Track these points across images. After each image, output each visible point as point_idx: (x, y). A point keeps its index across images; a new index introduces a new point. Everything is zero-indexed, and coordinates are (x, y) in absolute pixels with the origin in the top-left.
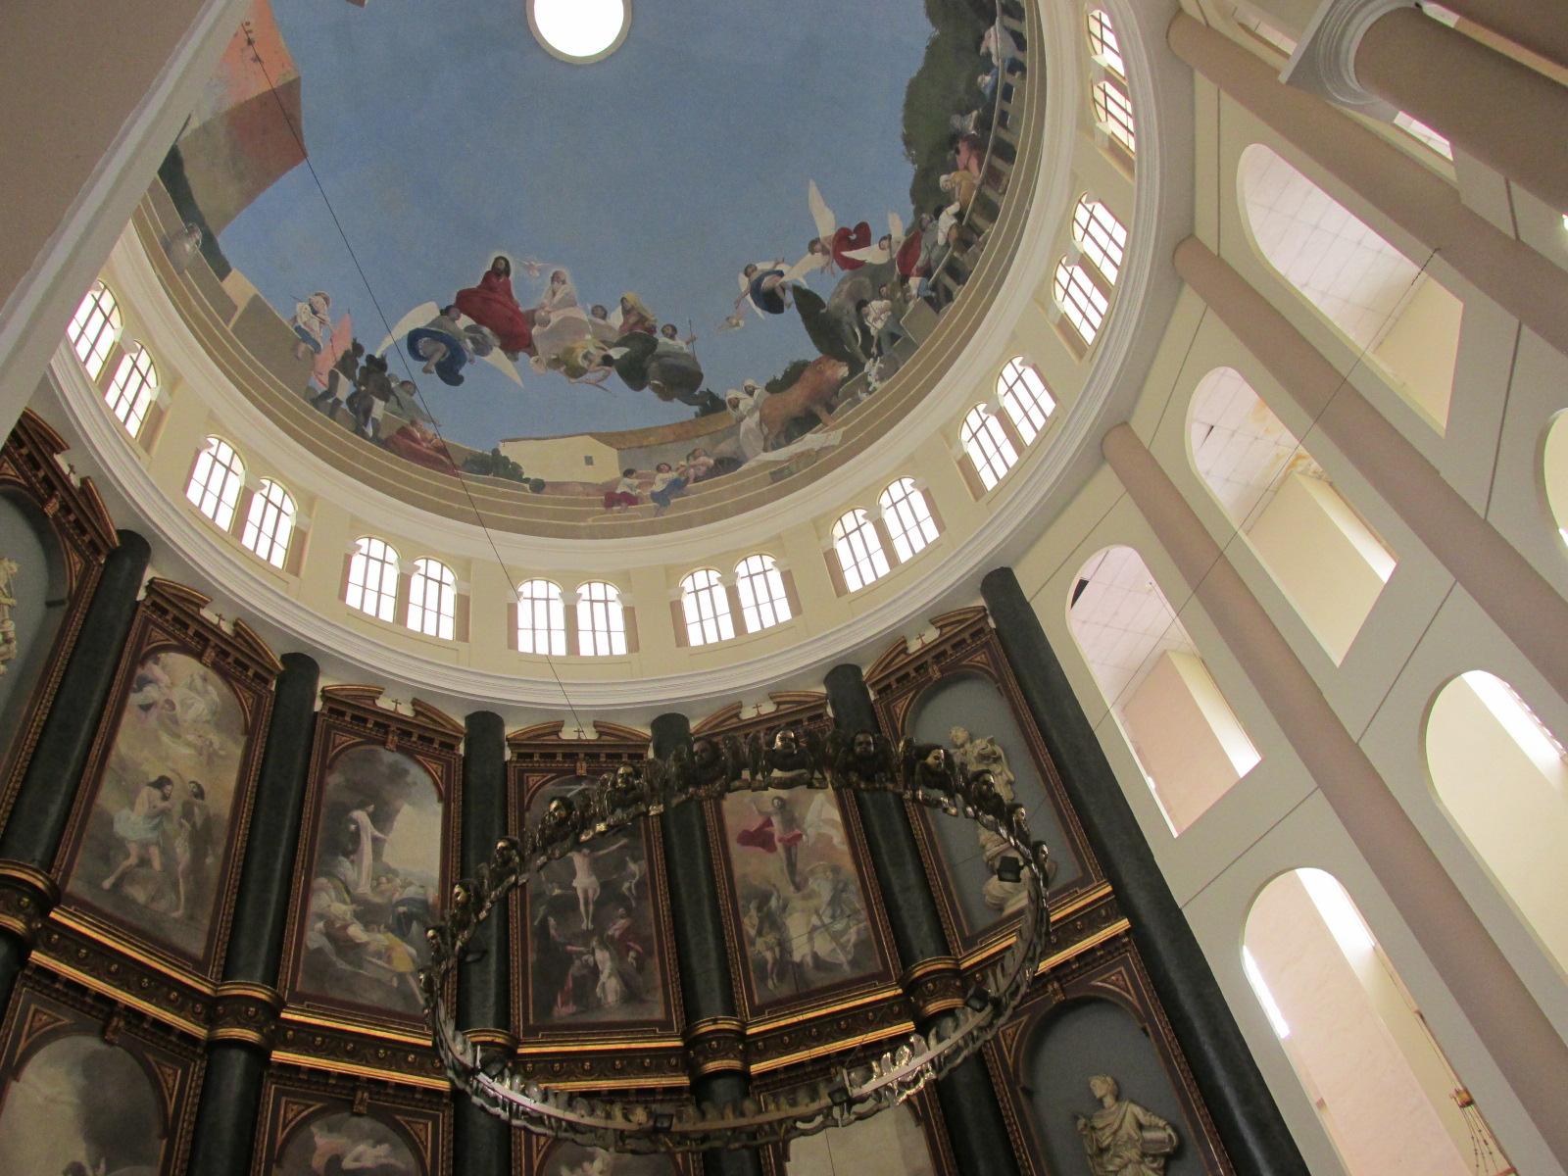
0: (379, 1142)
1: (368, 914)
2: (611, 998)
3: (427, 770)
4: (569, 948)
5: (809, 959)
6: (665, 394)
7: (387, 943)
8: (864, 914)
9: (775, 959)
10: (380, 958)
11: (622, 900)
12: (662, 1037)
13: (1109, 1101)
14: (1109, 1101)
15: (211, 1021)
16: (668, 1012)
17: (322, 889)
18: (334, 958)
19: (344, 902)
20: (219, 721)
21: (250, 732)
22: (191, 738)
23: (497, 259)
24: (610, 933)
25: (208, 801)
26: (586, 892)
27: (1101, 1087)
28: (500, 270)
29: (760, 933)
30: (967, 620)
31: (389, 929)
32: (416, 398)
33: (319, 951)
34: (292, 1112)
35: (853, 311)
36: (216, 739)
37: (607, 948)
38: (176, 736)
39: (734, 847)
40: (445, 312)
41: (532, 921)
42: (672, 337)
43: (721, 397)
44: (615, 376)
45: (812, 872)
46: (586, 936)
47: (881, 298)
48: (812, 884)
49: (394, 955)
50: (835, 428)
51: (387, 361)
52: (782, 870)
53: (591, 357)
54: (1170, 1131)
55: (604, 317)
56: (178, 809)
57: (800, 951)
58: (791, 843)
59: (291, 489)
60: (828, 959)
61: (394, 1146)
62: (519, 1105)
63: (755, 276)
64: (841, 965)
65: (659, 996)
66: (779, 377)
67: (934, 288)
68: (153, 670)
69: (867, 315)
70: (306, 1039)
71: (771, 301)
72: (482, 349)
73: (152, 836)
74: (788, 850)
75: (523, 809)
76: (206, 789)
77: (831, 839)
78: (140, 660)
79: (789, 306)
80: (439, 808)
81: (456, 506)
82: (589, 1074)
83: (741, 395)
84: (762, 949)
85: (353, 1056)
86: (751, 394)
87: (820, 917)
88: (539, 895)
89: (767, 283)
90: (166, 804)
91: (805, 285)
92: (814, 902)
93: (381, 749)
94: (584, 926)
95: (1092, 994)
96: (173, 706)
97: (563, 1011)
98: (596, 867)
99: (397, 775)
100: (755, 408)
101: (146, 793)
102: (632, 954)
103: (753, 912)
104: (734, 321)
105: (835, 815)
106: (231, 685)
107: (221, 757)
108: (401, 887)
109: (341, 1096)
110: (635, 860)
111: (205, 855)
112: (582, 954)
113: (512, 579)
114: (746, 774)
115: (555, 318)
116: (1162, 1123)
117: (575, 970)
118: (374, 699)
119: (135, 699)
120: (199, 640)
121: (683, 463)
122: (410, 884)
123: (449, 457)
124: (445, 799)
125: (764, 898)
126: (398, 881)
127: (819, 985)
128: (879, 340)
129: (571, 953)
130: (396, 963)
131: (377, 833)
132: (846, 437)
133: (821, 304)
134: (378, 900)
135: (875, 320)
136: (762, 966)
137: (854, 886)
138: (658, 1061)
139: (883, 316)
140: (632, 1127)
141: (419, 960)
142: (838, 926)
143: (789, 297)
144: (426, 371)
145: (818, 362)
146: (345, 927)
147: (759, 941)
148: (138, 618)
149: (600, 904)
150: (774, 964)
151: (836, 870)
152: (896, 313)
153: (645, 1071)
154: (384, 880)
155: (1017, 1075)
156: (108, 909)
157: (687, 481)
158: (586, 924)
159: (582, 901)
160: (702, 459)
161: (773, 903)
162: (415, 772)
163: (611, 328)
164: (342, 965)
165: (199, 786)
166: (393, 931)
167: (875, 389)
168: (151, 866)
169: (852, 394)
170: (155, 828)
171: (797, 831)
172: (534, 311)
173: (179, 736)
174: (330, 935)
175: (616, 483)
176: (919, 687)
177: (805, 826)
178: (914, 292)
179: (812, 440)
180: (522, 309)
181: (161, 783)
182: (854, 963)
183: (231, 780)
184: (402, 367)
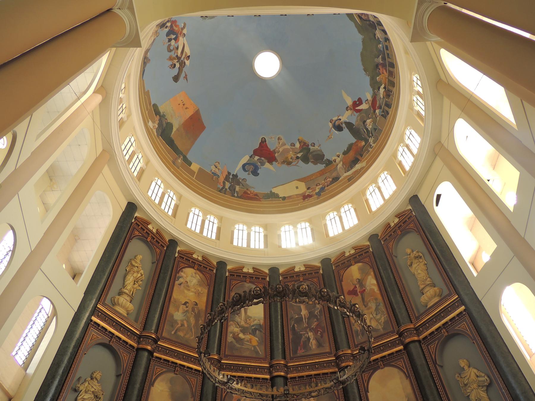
1: (244, 330)
2: (314, 347)
6: (315, 163)
7: (250, 338)
8: (385, 312)
9: (360, 329)
10: (248, 342)
11: (316, 316)
12: (329, 357)
13: (466, 368)
14: (466, 368)
17: (232, 325)
18: (236, 344)
20: (200, 284)
21: (209, 285)
22: (193, 290)
23: (262, 138)
24: (312, 327)
26: (305, 315)
27: (463, 363)
28: (263, 141)
30: (406, 214)
31: (250, 334)
32: (247, 182)
33: (231, 342)
35: (363, 125)
36: (200, 289)
37: (312, 332)
40: (251, 157)
41: (290, 326)
42: (314, 146)
43: (331, 160)
44: (300, 161)
45: (369, 301)
47: (370, 119)
49: (252, 341)
50: (363, 161)
51: (238, 175)
52: (361, 302)
53: (292, 158)
54: (486, 377)
55: (294, 146)
56: (190, 310)
58: (362, 292)
59: (216, 216)
62: (243, 390)
63: (333, 122)
64: (380, 329)
65: (328, 344)
66: (346, 150)
67: (383, 112)
68: (182, 274)
69: (367, 125)
71: (339, 128)
72: (263, 164)
73: (184, 318)
74: (362, 295)
77: (374, 289)
79: (344, 128)
81: (262, 210)
82: (308, 370)
83: (336, 158)
85: (242, 371)
86: (339, 157)
87: (373, 315)
88: (292, 318)
89: (337, 123)
90: (187, 309)
91: (348, 121)
92: (370, 310)
93: (245, 283)
95: (455, 332)
97: (301, 352)
98: (307, 308)
100: (341, 161)
101: (181, 306)
102: (319, 332)
104: (330, 137)
105: (375, 282)
106: (203, 274)
107: (202, 293)
108: (253, 321)
114: (247, 302)
115: (281, 150)
116: (483, 375)
117: (303, 339)
118: (242, 270)
121: (323, 182)
122: (256, 320)
123: (258, 196)
126: (252, 320)
128: (371, 131)
129: (301, 334)
132: (367, 163)
133: (354, 125)
134: (246, 326)
135: (369, 126)
136: (357, 331)
137: (382, 304)
139: (371, 124)
141: (259, 341)
142: (378, 317)
143: (344, 125)
144: (249, 174)
145: (356, 142)
147: (355, 324)
148: (176, 261)
150: (360, 332)
152: (374, 122)
153: (325, 368)
154: (248, 320)
155: (436, 361)
156: (174, 339)
157: (325, 187)
158: (305, 325)
160: (328, 179)
163: (297, 148)
164: (238, 345)
165: (196, 302)
166: (251, 334)
167: (373, 146)
168: (184, 326)
169: (367, 150)
170: (184, 316)
171: (364, 289)
172: (275, 149)
174: (234, 338)
175: (305, 192)
176: (395, 238)
177: (366, 287)
178: (378, 114)
179: (358, 166)
180: (271, 150)
181: (186, 303)
182: (384, 329)
183: (205, 299)
184: (242, 175)
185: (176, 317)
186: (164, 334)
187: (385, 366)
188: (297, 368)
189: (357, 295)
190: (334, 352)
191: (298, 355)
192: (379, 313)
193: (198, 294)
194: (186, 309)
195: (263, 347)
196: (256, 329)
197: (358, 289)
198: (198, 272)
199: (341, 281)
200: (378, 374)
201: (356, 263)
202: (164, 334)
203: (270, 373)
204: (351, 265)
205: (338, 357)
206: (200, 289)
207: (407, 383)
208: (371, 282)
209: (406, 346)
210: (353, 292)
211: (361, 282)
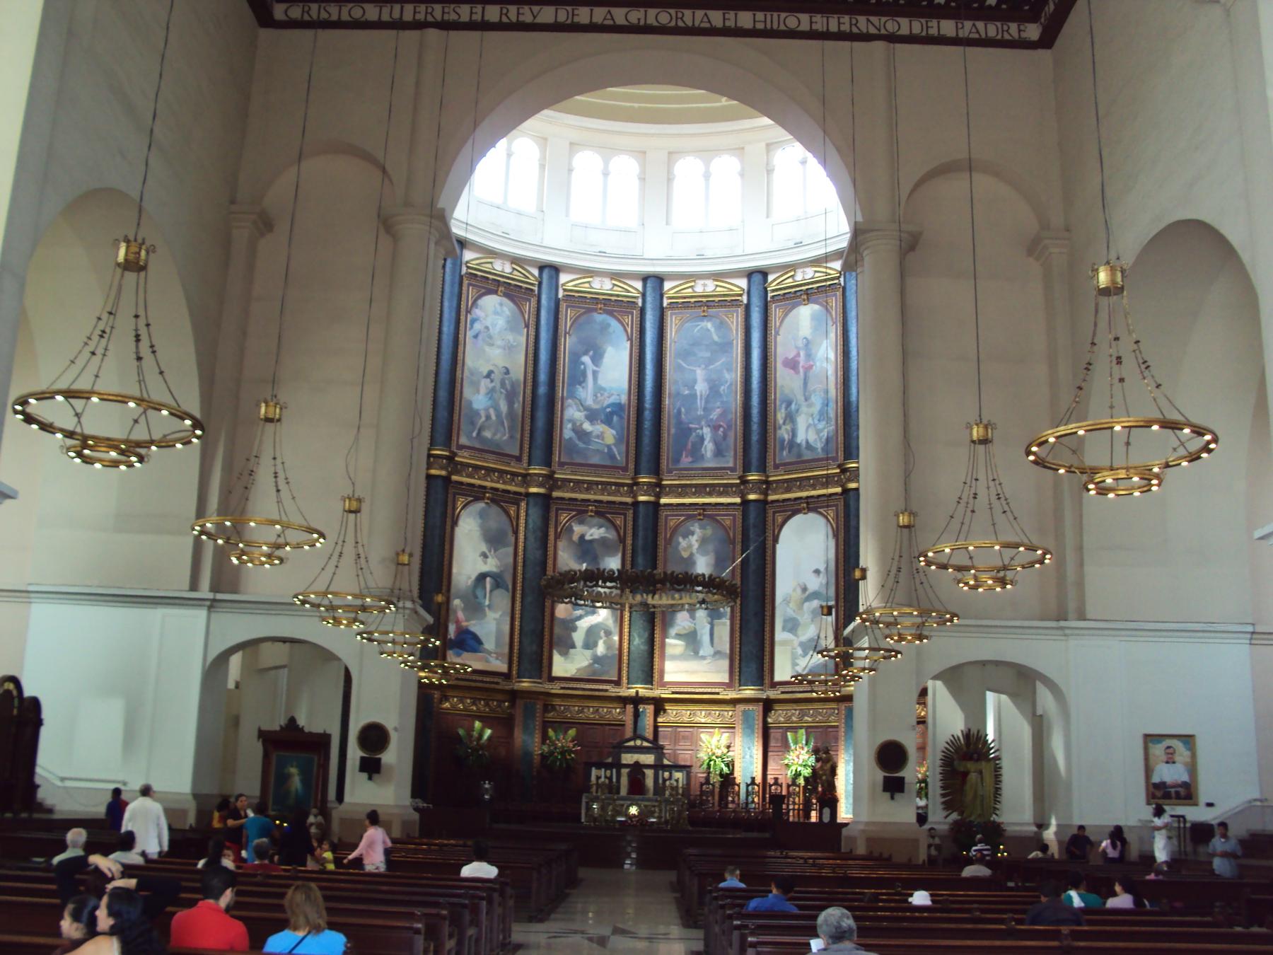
0: (601, 527)
1: (592, 416)
4: (691, 426)
5: (804, 443)
7: (601, 430)
8: (833, 422)
16: (735, 463)
17: (569, 406)
19: (580, 411)
20: (512, 327)
21: (527, 326)
24: (711, 417)
26: (701, 392)
29: (784, 423)
33: (570, 439)
36: (510, 337)
39: (779, 365)
46: (699, 419)
48: (813, 399)
49: (605, 435)
56: (498, 386)
57: (801, 438)
58: (808, 369)
60: (813, 444)
61: (607, 528)
68: (477, 312)
73: (489, 403)
76: (507, 366)
78: (468, 312)
80: (628, 344)
81: (636, 105)
84: (784, 433)
87: (813, 419)
88: (678, 394)
90: (493, 384)
94: (699, 413)
96: (487, 328)
97: (686, 461)
99: (605, 328)
102: (721, 429)
103: (783, 410)
105: (832, 356)
110: (729, 370)
111: (514, 403)
112: (697, 429)
117: (693, 437)
119: (470, 334)
122: (612, 395)
125: (789, 404)
126: (606, 394)
127: (805, 458)
129: (690, 429)
130: (606, 440)
131: (595, 368)
136: (784, 440)
140: (636, 602)
142: (821, 426)
146: (581, 424)
153: (720, 494)
154: (599, 395)
156: (477, 446)
158: (700, 412)
159: (699, 397)
161: (793, 406)
164: (581, 445)
165: (506, 368)
170: (490, 398)
171: (811, 363)
173: (493, 345)
174: (573, 430)
181: (489, 375)
182: (825, 449)
185: (476, 406)
187: (810, 510)
189: (797, 372)
190: (739, 472)
191: (682, 466)
192: (824, 419)
193: (509, 348)
194: (491, 385)
195: (623, 448)
196: (612, 414)
197: (802, 359)
198: (505, 300)
200: (798, 519)
202: (463, 440)
205: (744, 482)
207: (832, 543)
209: (846, 491)
210: (792, 364)
211: (808, 343)
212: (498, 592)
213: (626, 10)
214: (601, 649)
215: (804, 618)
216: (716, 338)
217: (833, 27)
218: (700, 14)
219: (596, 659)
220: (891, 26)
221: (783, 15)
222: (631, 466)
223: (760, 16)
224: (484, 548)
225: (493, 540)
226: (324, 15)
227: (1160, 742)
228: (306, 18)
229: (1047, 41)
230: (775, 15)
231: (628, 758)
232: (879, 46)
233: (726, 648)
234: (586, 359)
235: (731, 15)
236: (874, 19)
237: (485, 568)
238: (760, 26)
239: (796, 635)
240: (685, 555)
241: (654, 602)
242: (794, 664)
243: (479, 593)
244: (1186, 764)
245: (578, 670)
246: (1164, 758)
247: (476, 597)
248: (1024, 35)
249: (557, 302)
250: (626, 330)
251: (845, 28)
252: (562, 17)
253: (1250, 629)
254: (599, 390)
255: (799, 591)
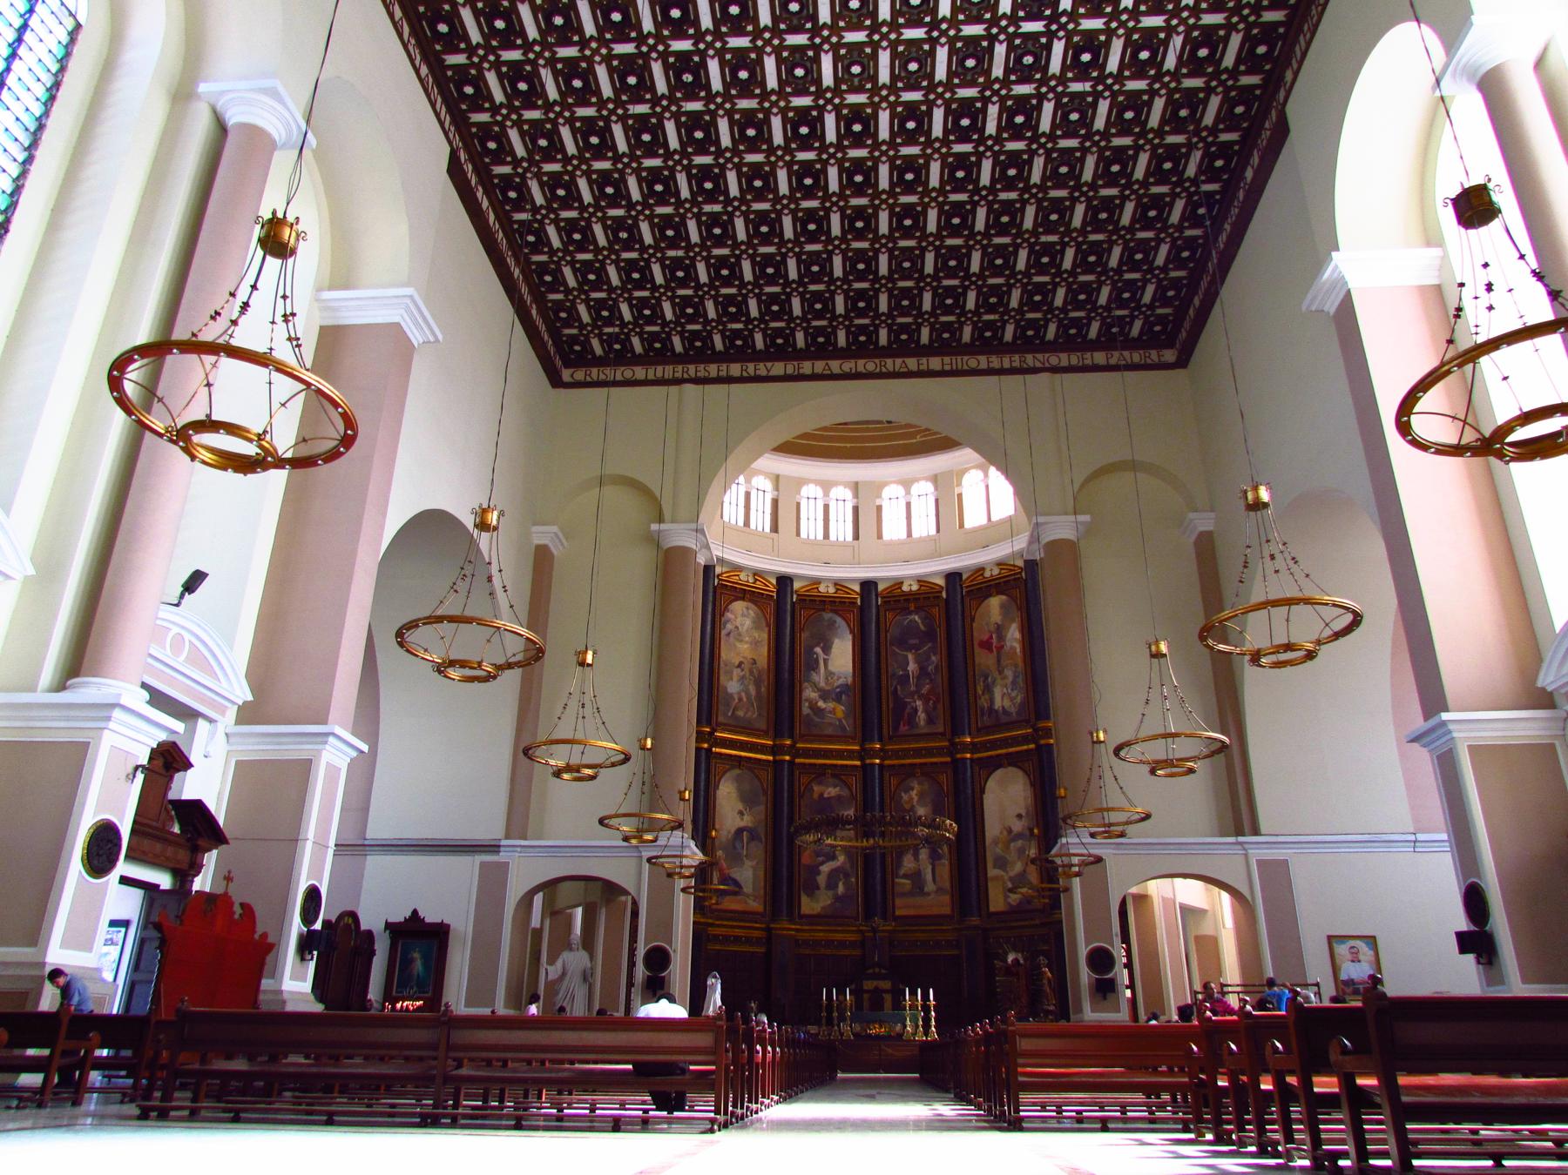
0: (835, 786)
1: (825, 695)
2: (922, 723)
3: (844, 619)
11: (928, 674)
15: (774, 755)
21: (768, 625)
25: (759, 664)
34: (805, 779)
36: (756, 635)
38: (741, 641)
39: (976, 646)
46: (912, 694)
57: (998, 704)
68: (729, 615)
70: (808, 753)
74: (998, 652)
75: (886, 631)
78: (722, 615)
80: (850, 637)
84: (983, 702)
88: (894, 675)
97: (903, 729)
98: (917, 661)
99: (832, 624)
105: (1017, 635)
109: (820, 773)
113: (878, 487)
117: (908, 710)
119: (723, 632)
120: (743, 593)
122: (839, 678)
124: (852, 632)
125: (986, 678)
134: (827, 688)
138: (939, 751)
142: (1014, 694)
149: (919, 678)
151: (1016, 666)
153: (934, 756)
156: (731, 722)
158: (913, 688)
162: (839, 620)
164: (817, 720)
181: (739, 665)
182: (1017, 713)
183: (764, 650)
185: (729, 690)
186: (721, 719)
187: (1010, 764)
188: (896, 754)
195: (851, 721)
196: (841, 693)
197: (994, 640)
198: (750, 604)
199: (973, 620)
200: (999, 773)
201: (999, 593)
202: (721, 719)
203: (862, 759)
204: (990, 595)
205: (953, 744)
206: (756, 635)
207: (1029, 792)
208: (1014, 634)
209: (1039, 747)
210: (986, 645)
212: (753, 844)
213: (840, 362)
214: (841, 889)
215: (1012, 856)
216: (922, 627)
217: (1006, 365)
218: (899, 361)
219: (837, 898)
220: (1054, 360)
221: (966, 358)
222: (859, 735)
223: (947, 359)
224: (740, 806)
225: (748, 799)
226: (602, 377)
227: (1343, 943)
228: (588, 379)
229: (1182, 362)
230: (959, 358)
231: (869, 985)
232: (1045, 376)
233: (947, 885)
234: (818, 650)
235: (924, 360)
236: (1039, 356)
237: (743, 824)
238: (947, 368)
239: (1005, 870)
240: (907, 807)
241: (886, 844)
242: (1006, 897)
243: (738, 845)
244: (1370, 962)
245: (823, 908)
246: (1349, 957)
247: (735, 848)
248: (1162, 359)
249: (793, 604)
250: (849, 626)
251: (1016, 364)
252: (790, 370)
253: (1412, 838)
254: (829, 674)
255: (1005, 833)
